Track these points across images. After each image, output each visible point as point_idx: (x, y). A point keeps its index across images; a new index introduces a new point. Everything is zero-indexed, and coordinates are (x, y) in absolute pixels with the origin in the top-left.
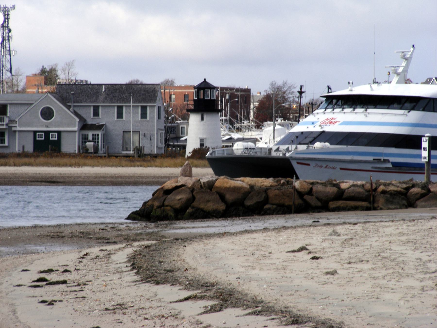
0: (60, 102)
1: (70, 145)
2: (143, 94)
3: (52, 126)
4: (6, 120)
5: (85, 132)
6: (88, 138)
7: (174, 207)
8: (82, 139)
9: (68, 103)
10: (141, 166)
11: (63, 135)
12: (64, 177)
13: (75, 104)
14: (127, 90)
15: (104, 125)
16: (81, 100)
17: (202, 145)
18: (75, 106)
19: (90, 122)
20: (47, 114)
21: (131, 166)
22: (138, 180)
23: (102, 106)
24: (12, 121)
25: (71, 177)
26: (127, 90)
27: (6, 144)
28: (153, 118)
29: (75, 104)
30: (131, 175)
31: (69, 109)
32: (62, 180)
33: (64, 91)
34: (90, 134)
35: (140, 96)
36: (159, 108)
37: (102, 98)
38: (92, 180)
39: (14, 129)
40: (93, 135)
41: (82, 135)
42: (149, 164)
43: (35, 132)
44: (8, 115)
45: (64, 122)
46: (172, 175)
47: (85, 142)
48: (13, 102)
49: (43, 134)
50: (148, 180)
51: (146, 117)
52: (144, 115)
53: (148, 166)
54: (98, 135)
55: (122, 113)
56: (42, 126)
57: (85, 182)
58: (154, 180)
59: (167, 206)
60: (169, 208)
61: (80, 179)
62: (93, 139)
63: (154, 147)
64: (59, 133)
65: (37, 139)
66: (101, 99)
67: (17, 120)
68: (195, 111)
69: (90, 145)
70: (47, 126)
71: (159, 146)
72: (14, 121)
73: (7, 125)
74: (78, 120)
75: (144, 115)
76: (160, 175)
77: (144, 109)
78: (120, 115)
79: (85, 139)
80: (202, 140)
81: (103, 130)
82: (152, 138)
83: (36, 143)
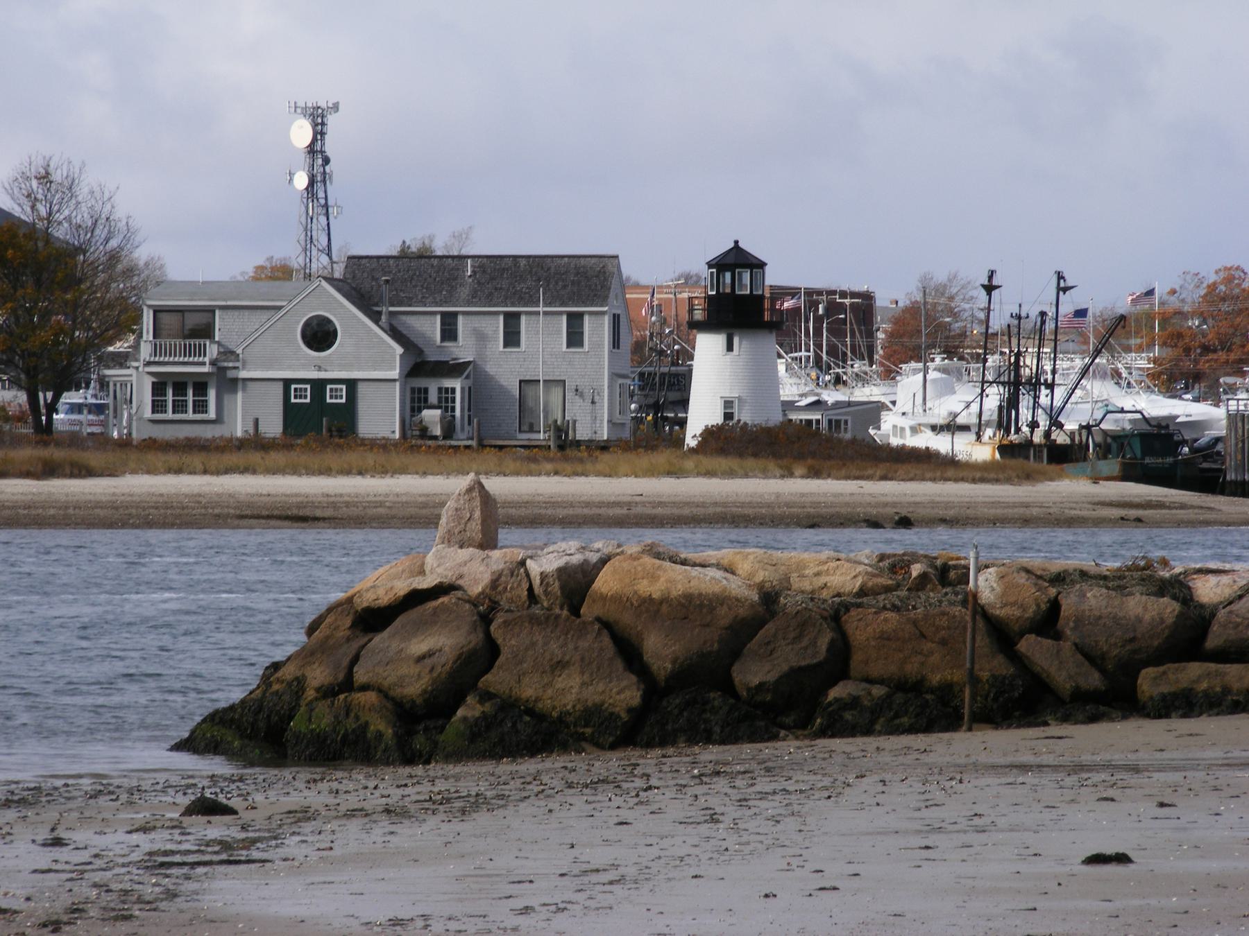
0: (353, 303)
1: (380, 416)
2: (573, 282)
3: (333, 365)
4: (212, 351)
5: (421, 383)
6: (426, 400)
7: (397, 692)
8: (413, 400)
9: (377, 305)
10: (556, 473)
11: (361, 388)
12: (334, 505)
13: (391, 309)
14: (530, 272)
15: (469, 362)
16: (411, 299)
17: (728, 416)
18: (391, 313)
19: (432, 357)
20: (319, 335)
21: (530, 473)
22: (543, 511)
23: (464, 313)
24: (228, 353)
25: (355, 505)
26: (530, 272)
27: (212, 414)
28: (601, 345)
29: (391, 309)
30: (526, 498)
31: (377, 322)
32: (328, 513)
33: (365, 275)
34: (433, 387)
35: (565, 287)
36: (616, 320)
37: (464, 292)
38: (413, 511)
39: (231, 374)
40: (440, 389)
41: (413, 390)
42: (579, 468)
43: (287, 383)
44: (217, 339)
45: (367, 358)
46: (638, 499)
47: (420, 411)
48: (229, 303)
49: (308, 387)
50: (571, 512)
51: (581, 344)
52: (575, 338)
53: (576, 474)
54: (453, 390)
55: (519, 333)
56: (304, 367)
57: (393, 517)
58: (586, 511)
59: (364, 688)
60: (371, 697)
61: (381, 510)
62: (440, 399)
63: (602, 421)
64: (352, 384)
65: (293, 400)
66: (463, 296)
67: (239, 351)
68: (708, 325)
69: (432, 416)
70: (320, 369)
71: (615, 421)
72: (233, 353)
73: (213, 363)
74: (399, 350)
75: (575, 338)
76: (604, 499)
77: (575, 321)
78: (512, 338)
79: (417, 400)
80: (728, 404)
81: (467, 377)
82: (597, 398)
83: (290, 411)
